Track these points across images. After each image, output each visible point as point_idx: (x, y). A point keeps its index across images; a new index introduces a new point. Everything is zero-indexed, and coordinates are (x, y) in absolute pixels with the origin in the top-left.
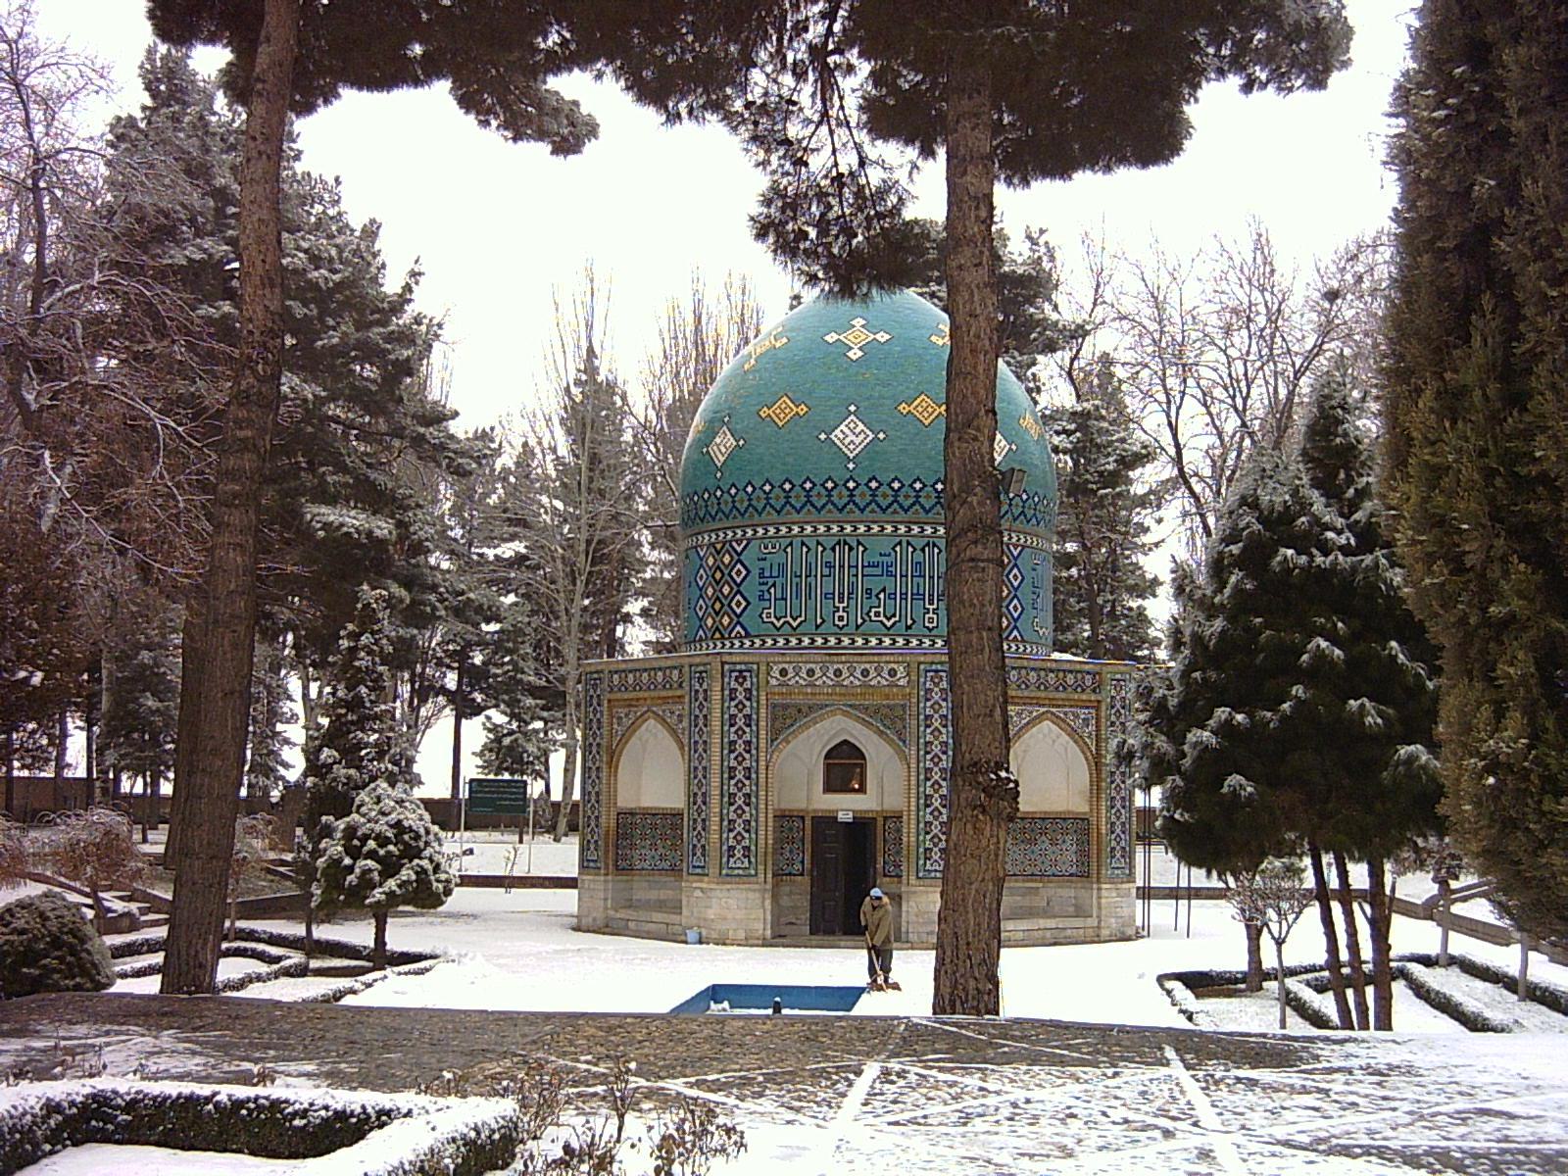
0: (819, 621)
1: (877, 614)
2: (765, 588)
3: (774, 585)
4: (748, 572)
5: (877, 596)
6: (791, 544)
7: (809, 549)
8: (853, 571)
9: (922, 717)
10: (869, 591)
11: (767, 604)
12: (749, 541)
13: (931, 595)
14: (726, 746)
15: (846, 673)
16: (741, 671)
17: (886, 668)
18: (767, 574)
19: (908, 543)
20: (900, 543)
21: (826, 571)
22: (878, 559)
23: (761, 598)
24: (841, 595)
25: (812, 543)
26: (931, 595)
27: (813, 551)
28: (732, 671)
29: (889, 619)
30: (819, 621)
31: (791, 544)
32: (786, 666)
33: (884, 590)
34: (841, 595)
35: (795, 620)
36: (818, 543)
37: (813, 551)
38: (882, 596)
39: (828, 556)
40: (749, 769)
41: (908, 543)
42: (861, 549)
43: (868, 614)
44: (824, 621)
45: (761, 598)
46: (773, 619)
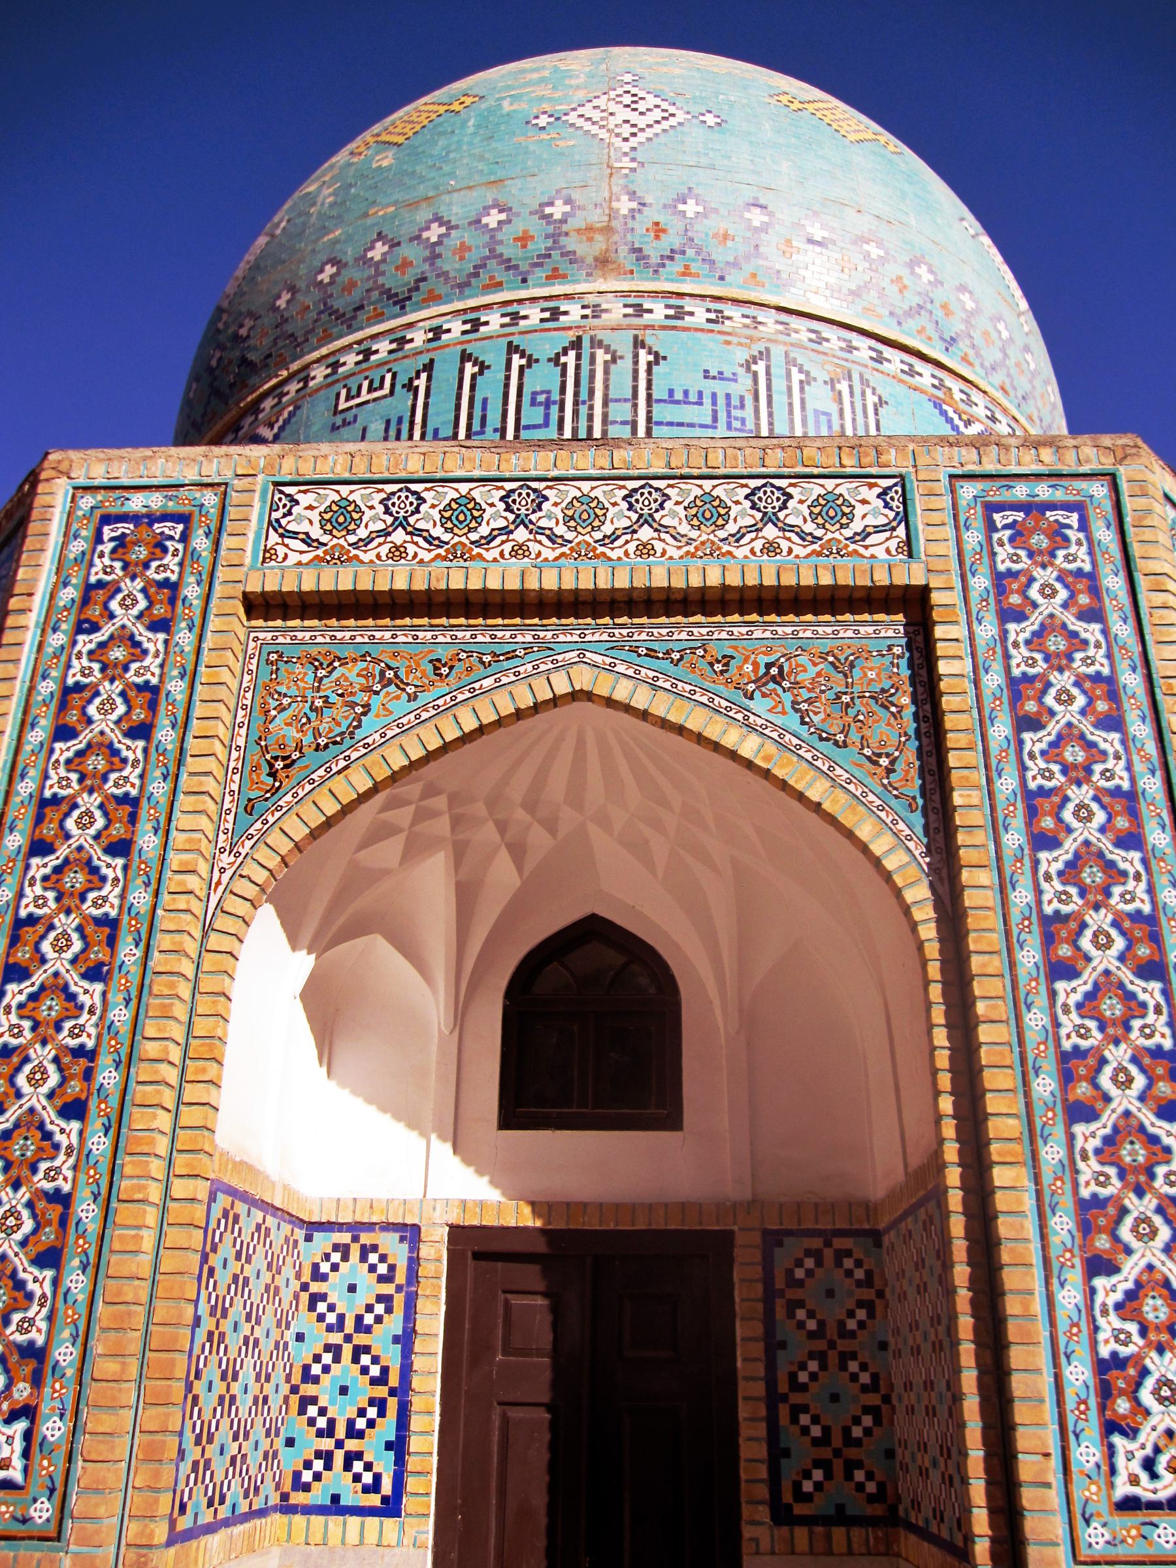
6: (429, 367)
7: (483, 367)
8: (621, 412)
19: (790, 362)
20: (765, 355)
21: (533, 415)
22: (697, 383)
25: (494, 355)
27: (495, 376)
31: (429, 367)
32: (358, 495)
36: (512, 349)
37: (495, 376)
39: (543, 378)
40: (111, 925)
41: (790, 362)
42: (644, 357)
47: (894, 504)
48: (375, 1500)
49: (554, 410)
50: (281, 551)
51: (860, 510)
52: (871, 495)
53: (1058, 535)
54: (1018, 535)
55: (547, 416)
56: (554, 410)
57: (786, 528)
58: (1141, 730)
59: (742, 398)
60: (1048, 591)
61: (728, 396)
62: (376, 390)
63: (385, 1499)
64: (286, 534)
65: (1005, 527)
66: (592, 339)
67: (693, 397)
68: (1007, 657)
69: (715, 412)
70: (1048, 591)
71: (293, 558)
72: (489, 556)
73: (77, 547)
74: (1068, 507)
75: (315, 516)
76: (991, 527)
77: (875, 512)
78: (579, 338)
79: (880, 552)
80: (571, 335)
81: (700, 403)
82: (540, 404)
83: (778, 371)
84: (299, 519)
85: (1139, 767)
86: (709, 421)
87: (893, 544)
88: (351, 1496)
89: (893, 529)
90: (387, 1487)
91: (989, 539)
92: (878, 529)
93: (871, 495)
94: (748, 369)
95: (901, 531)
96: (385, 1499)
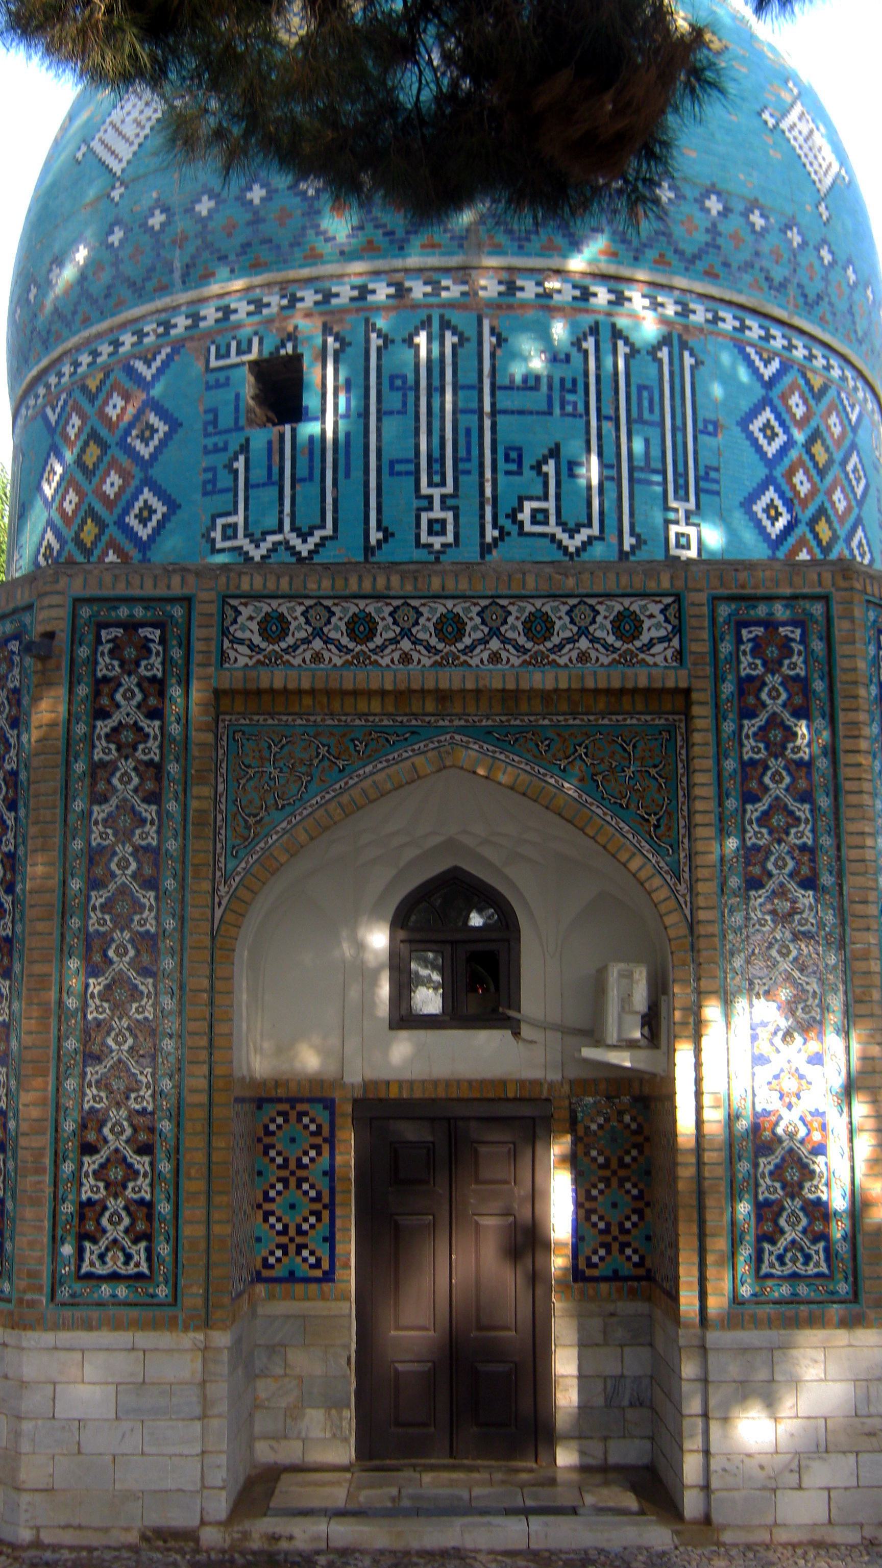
0: (375, 536)
1: (539, 517)
2: (220, 460)
3: (245, 448)
4: (174, 425)
5: (537, 467)
9: (730, 765)
10: (514, 456)
11: (221, 501)
12: (178, 346)
13: (681, 475)
14: (80, 866)
15: (473, 620)
16: (131, 626)
17: (607, 611)
18: (226, 420)
21: (393, 400)
23: (210, 488)
24: (436, 461)
26: (681, 475)
28: (101, 626)
29: (572, 533)
30: (375, 536)
33: (555, 452)
34: (436, 461)
35: (303, 537)
38: (550, 468)
43: (512, 516)
44: (388, 535)
45: (210, 488)
46: (242, 541)
47: (672, 619)
48: (318, 1273)
49: (411, 395)
50: (232, 654)
51: (647, 623)
52: (655, 609)
53: (786, 649)
54: (758, 649)
55: (405, 404)
56: (411, 395)
57: (593, 640)
58: (824, 802)
59: (574, 381)
60: (774, 694)
61: (562, 380)
62: (244, 353)
63: (325, 1273)
64: (236, 641)
65: (749, 640)
66: (442, 317)
67: (531, 382)
68: (741, 745)
69: (550, 398)
70: (774, 694)
71: (242, 661)
72: (385, 661)
73: (83, 652)
74: (795, 623)
75: (254, 626)
76: (739, 641)
77: (658, 626)
78: (429, 318)
79: (659, 660)
80: (423, 314)
81: (536, 388)
82: (398, 389)
83: (606, 346)
84: (243, 628)
85: (820, 830)
86: (544, 407)
87: (669, 653)
88: (303, 1270)
89: (670, 640)
90: (326, 1265)
91: (738, 649)
92: (661, 640)
93: (655, 609)
94: (580, 348)
95: (675, 642)
96: (325, 1273)
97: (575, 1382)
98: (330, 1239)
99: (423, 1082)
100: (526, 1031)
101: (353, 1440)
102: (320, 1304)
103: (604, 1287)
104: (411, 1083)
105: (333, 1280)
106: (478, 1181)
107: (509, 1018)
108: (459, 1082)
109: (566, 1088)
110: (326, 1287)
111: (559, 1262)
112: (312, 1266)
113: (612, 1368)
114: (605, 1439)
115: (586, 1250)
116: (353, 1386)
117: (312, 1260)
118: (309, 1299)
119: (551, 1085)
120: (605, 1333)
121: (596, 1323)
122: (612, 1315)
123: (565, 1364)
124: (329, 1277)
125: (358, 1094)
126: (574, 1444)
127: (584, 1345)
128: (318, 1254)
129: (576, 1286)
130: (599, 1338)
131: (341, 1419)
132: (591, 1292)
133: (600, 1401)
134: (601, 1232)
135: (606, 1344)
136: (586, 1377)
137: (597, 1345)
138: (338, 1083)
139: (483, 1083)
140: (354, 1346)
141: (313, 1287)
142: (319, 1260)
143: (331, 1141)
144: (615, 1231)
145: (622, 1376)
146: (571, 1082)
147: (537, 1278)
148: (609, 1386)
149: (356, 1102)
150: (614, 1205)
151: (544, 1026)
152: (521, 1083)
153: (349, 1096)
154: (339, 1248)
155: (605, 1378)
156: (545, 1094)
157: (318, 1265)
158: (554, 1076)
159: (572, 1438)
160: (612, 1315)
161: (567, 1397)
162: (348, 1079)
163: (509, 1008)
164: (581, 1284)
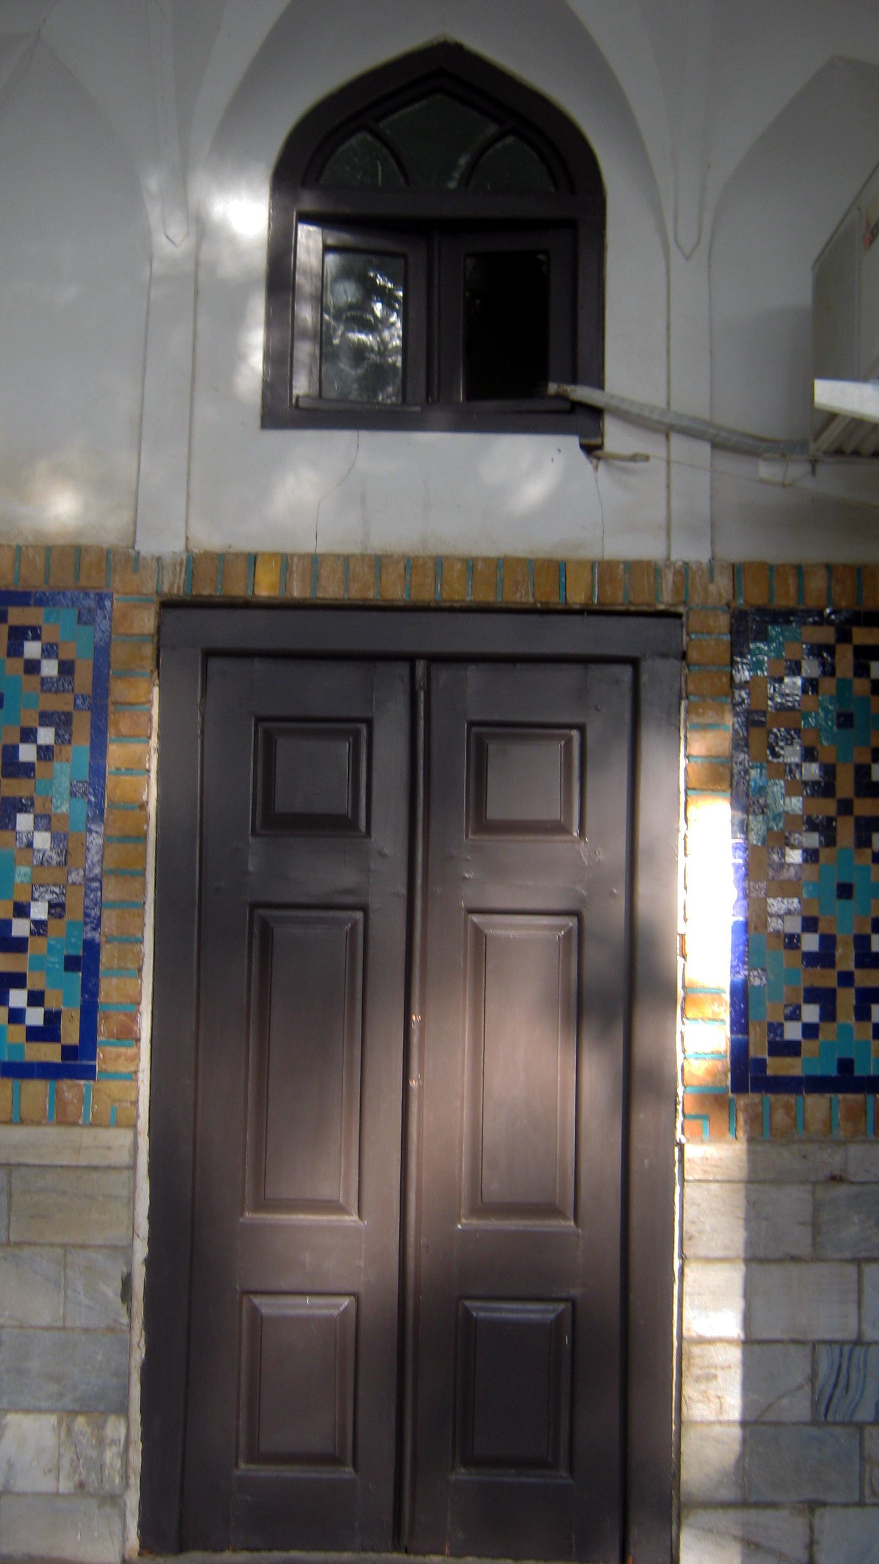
48: (50, 1053)
63: (69, 1052)
90: (71, 1033)
96: (69, 1052)
97: (735, 1355)
98: (85, 963)
99: (346, 559)
100: (616, 437)
101: (133, 1499)
102: (52, 1134)
103: (816, 1105)
104: (315, 561)
105: (89, 1073)
106: (482, 824)
107: (577, 406)
108: (440, 563)
109: (722, 584)
110: (69, 1088)
111: (700, 1042)
112: (34, 1034)
113: (832, 1320)
114: (812, 1506)
115: (769, 1010)
116: (139, 1355)
117: (35, 1017)
118: (22, 1122)
119: (685, 572)
120: (816, 1227)
121: (794, 1200)
122: (835, 1179)
123: (710, 1311)
124: (78, 1063)
125: (173, 584)
126: (728, 1520)
127: (762, 1259)
128: (52, 1003)
129: (742, 1101)
130: (801, 1241)
131: (101, 1443)
132: (780, 1117)
133: (798, 1408)
134: (811, 959)
135: (817, 1259)
136: (761, 1342)
137: (794, 1259)
138: (120, 559)
139: (503, 565)
140: (141, 1250)
141: (36, 1088)
142: (52, 1018)
143: (99, 706)
144: (845, 957)
145: (858, 1342)
146: (737, 571)
147: (639, 1083)
148: (824, 1368)
149: (168, 605)
150: (845, 891)
151: (666, 428)
152: (605, 570)
153: (150, 588)
154: (109, 989)
155: (815, 1344)
156: (666, 599)
157: (48, 1031)
158: (692, 551)
159: (725, 1505)
160: (835, 1179)
161: (713, 1402)
162: (147, 547)
163: (574, 381)
164: (752, 1098)
